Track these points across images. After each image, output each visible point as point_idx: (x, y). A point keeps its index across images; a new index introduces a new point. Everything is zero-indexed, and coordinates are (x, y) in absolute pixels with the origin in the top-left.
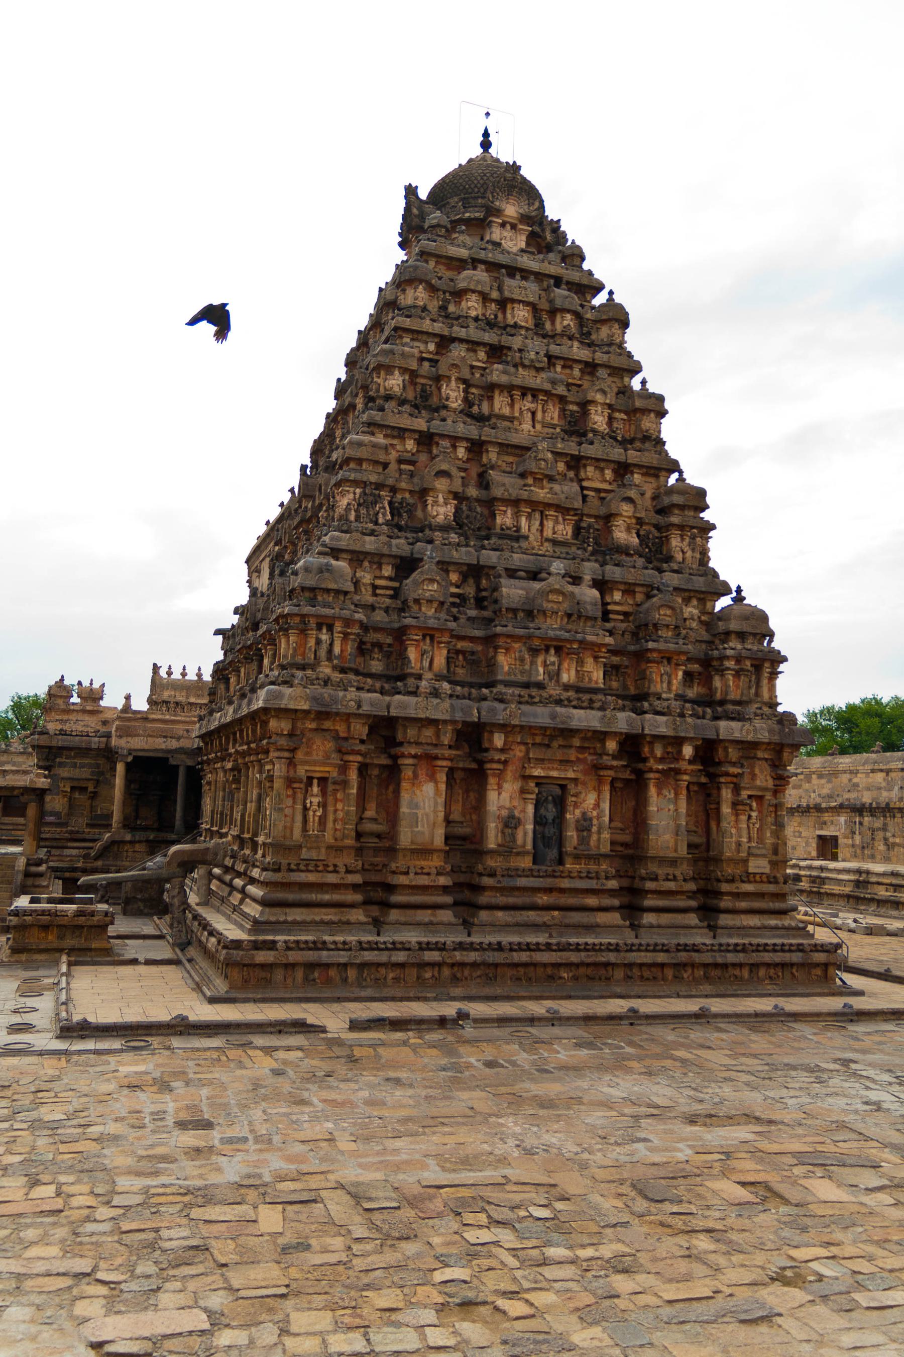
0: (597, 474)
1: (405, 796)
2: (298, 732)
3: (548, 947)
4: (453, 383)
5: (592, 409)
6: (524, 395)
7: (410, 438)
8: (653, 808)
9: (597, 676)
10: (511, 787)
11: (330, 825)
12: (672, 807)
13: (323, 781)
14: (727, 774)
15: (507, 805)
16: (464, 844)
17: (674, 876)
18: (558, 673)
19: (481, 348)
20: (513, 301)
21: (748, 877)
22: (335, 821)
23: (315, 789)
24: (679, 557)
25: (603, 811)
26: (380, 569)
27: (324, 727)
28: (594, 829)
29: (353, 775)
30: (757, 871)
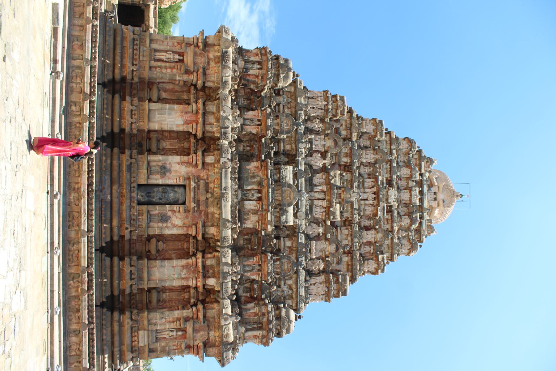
0: (345, 237)
1: (176, 106)
2: (207, 49)
3: (90, 185)
4: (373, 156)
5: (373, 232)
6: (374, 193)
7: (347, 133)
8: (175, 262)
9: (249, 224)
10: (183, 170)
11: (159, 64)
12: (176, 276)
13: (182, 61)
14: (198, 311)
15: (172, 169)
16: (147, 142)
17: (133, 279)
18: (247, 200)
19: (389, 175)
20: (410, 192)
21: (134, 330)
22: (160, 67)
23: (177, 57)
24: (313, 281)
25: (171, 229)
26: (288, 108)
27: (211, 62)
28: (160, 224)
29: (185, 77)
30: (140, 337)
